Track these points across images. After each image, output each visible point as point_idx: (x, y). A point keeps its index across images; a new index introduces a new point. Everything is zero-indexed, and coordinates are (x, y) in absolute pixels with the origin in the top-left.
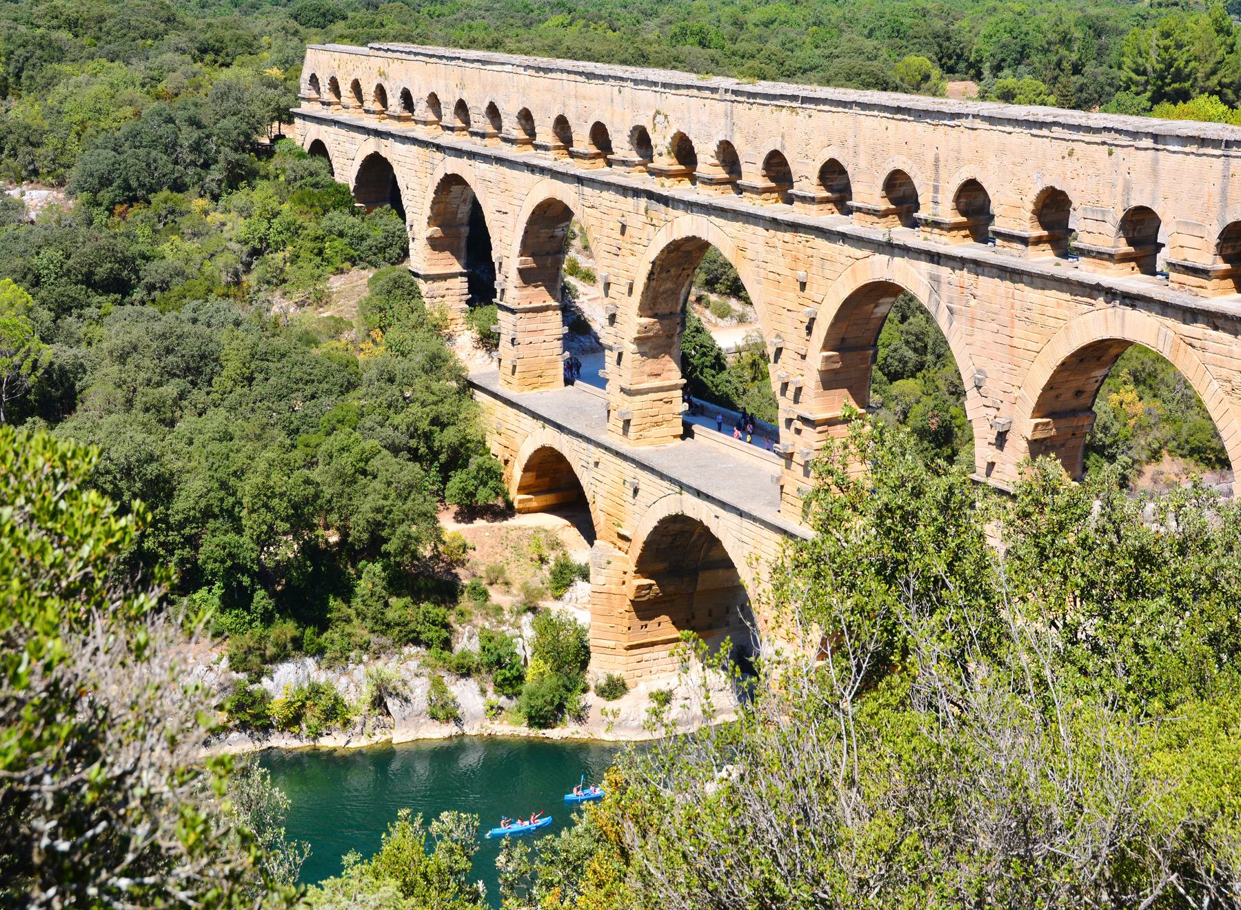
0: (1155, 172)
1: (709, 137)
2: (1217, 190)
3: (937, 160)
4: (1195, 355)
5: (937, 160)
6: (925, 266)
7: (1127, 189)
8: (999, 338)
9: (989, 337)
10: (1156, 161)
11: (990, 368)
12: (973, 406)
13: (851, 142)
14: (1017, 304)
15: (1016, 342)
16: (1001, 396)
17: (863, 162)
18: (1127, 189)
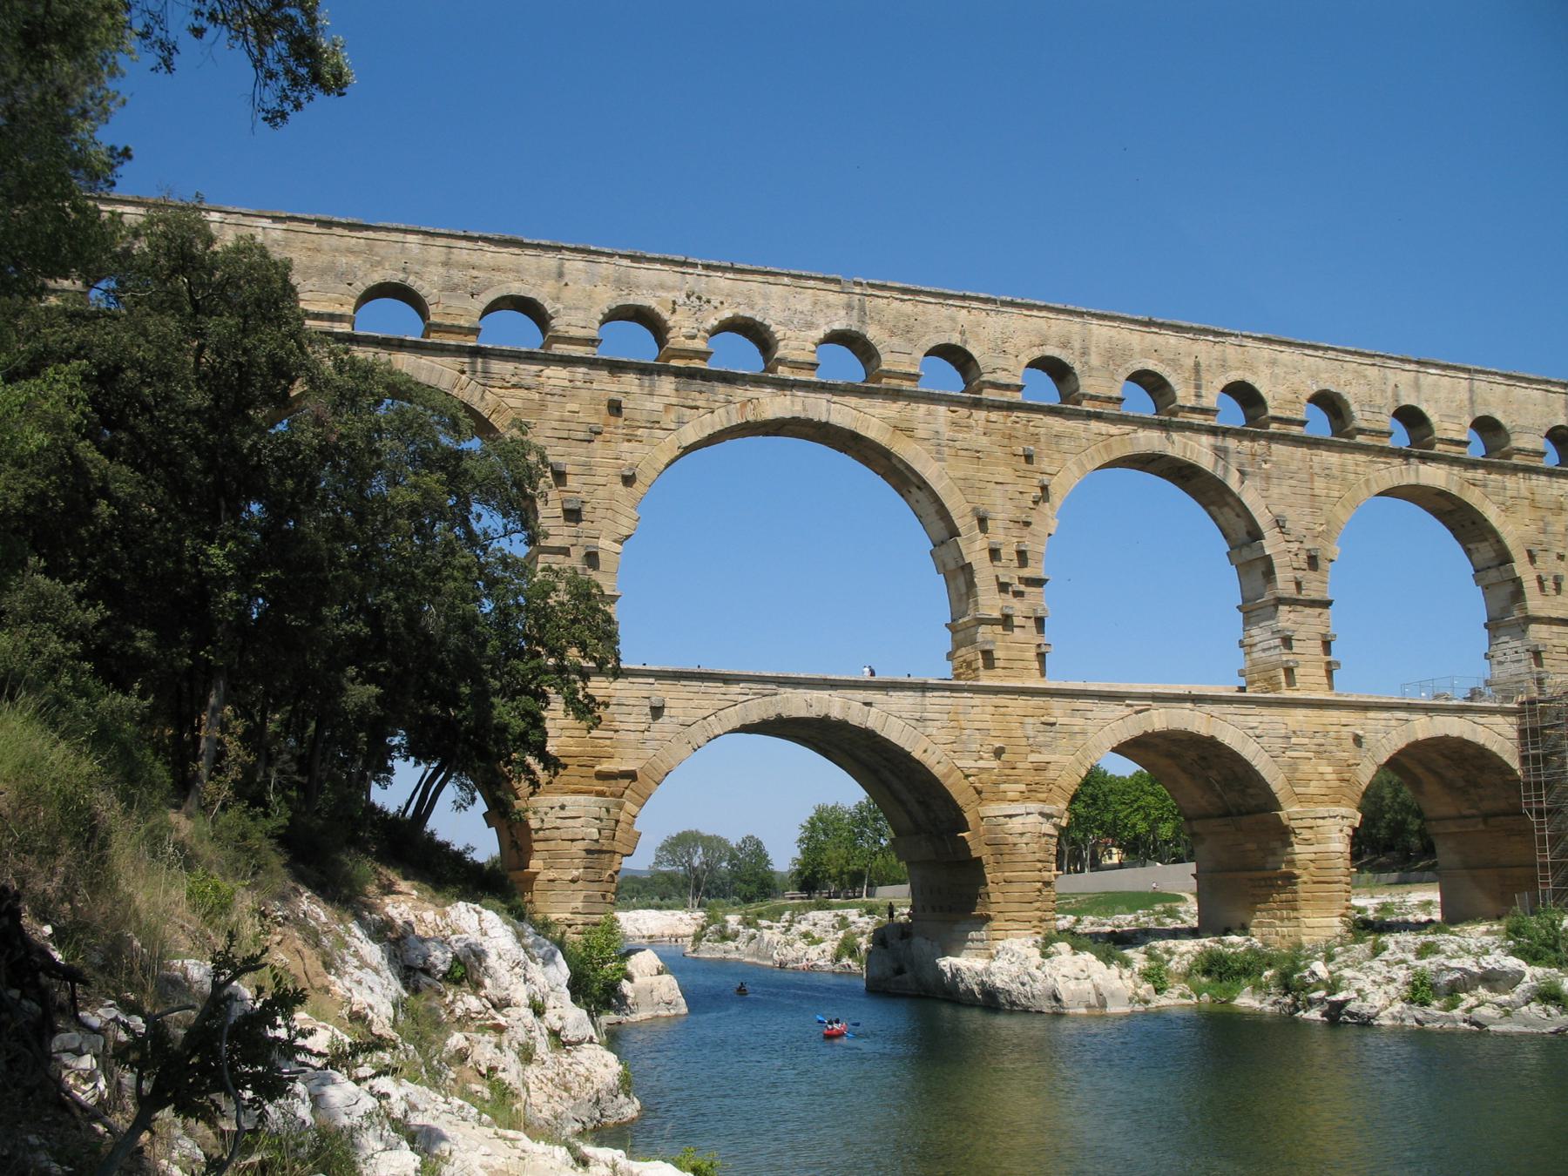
0: (1417, 386)
1: (810, 326)
2: (1466, 396)
3: (1197, 365)
4: (1477, 490)
5: (1197, 365)
6: (1206, 440)
7: (1396, 397)
8: (1298, 490)
9: (1286, 490)
10: (1417, 380)
11: (1291, 515)
12: (1272, 544)
13: (1077, 345)
14: (1316, 466)
15: (1317, 492)
16: (1304, 532)
17: (1095, 360)
18: (1396, 397)
